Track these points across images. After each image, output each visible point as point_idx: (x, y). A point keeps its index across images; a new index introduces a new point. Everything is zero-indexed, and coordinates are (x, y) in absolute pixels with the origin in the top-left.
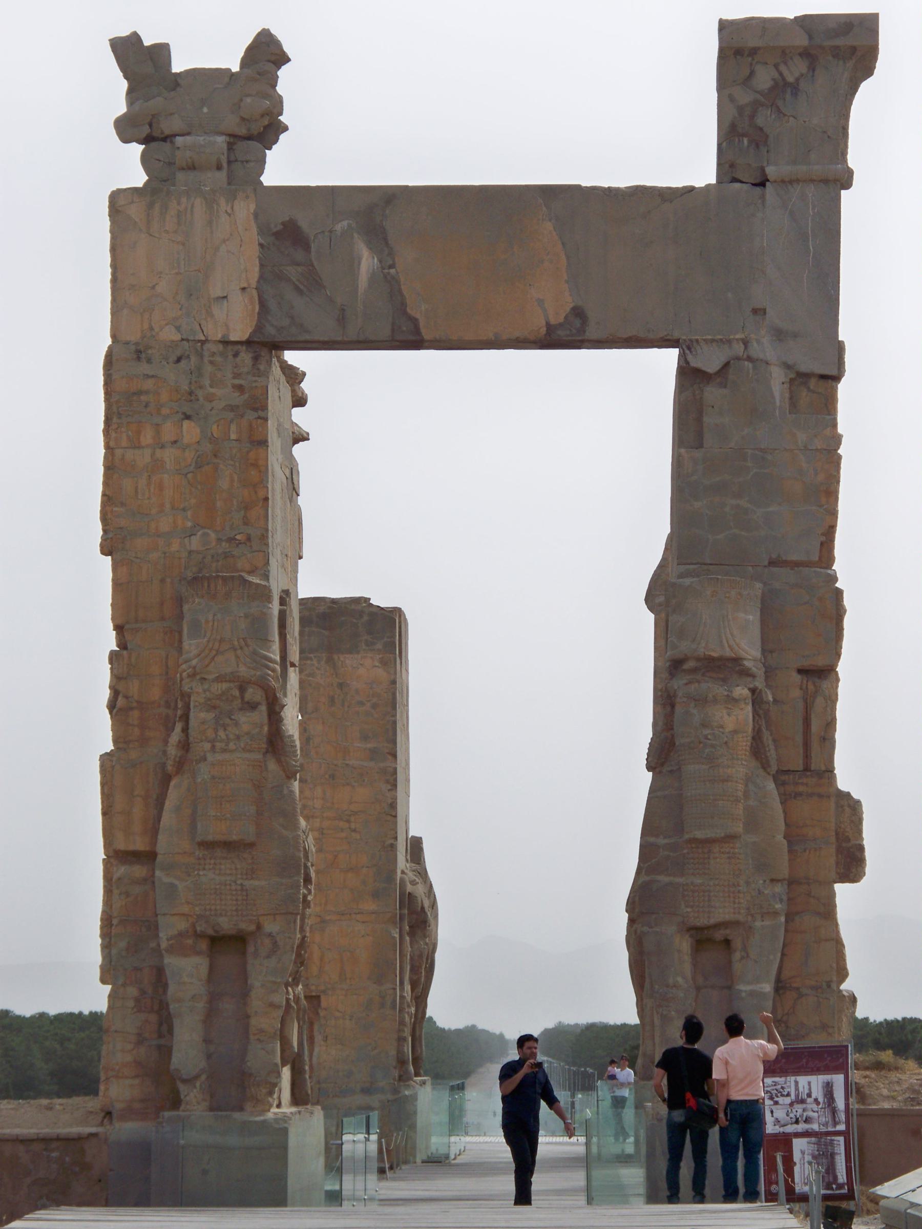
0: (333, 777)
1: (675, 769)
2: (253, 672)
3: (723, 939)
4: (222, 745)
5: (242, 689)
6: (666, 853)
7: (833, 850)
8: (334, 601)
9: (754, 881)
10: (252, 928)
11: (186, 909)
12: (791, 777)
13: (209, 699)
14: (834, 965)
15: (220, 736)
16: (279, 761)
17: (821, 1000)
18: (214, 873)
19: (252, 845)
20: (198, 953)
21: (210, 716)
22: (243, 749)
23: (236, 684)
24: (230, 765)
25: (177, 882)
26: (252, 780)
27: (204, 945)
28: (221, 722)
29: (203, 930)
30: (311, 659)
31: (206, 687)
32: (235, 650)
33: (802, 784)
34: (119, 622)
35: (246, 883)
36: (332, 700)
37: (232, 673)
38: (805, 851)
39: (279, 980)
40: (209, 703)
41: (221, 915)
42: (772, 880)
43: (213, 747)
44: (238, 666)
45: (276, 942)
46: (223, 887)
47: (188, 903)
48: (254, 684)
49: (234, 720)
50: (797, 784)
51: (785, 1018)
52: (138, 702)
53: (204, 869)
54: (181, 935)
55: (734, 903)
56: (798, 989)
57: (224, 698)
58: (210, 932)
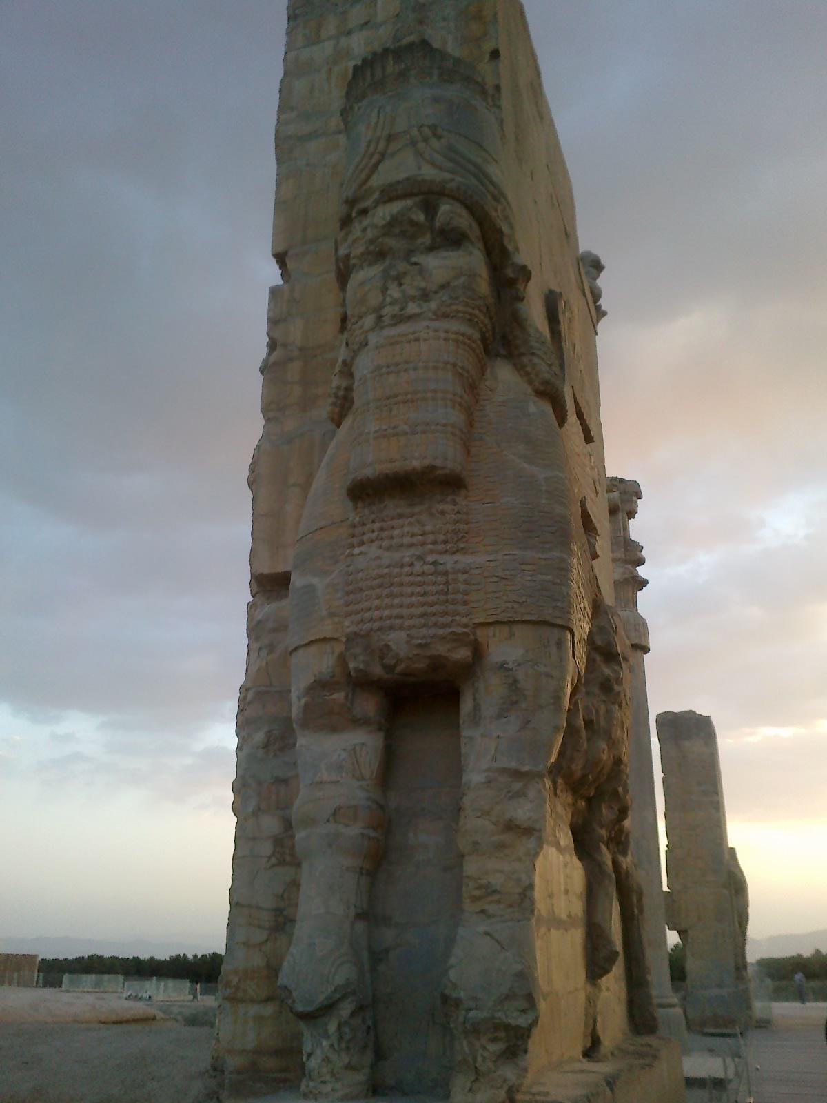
2: (447, 176)
4: (396, 309)
5: (430, 209)
8: (676, 713)
10: (463, 654)
11: (327, 630)
13: (372, 241)
15: (390, 296)
16: (520, 368)
18: (380, 547)
19: (452, 483)
20: (358, 722)
21: (375, 271)
22: (435, 313)
23: (417, 199)
24: (409, 342)
25: (315, 581)
26: (455, 365)
27: (369, 705)
28: (393, 273)
29: (361, 666)
31: (366, 222)
32: (413, 143)
34: (280, 249)
35: (449, 561)
37: (408, 179)
39: (526, 768)
40: (372, 248)
41: (391, 628)
43: (380, 318)
44: (420, 168)
45: (516, 681)
46: (396, 571)
47: (332, 615)
48: (449, 196)
49: (416, 264)
52: (301, 349)
53: (362, 543)
54: (321, 685)
57: (397, 230)
58: (377, 671)
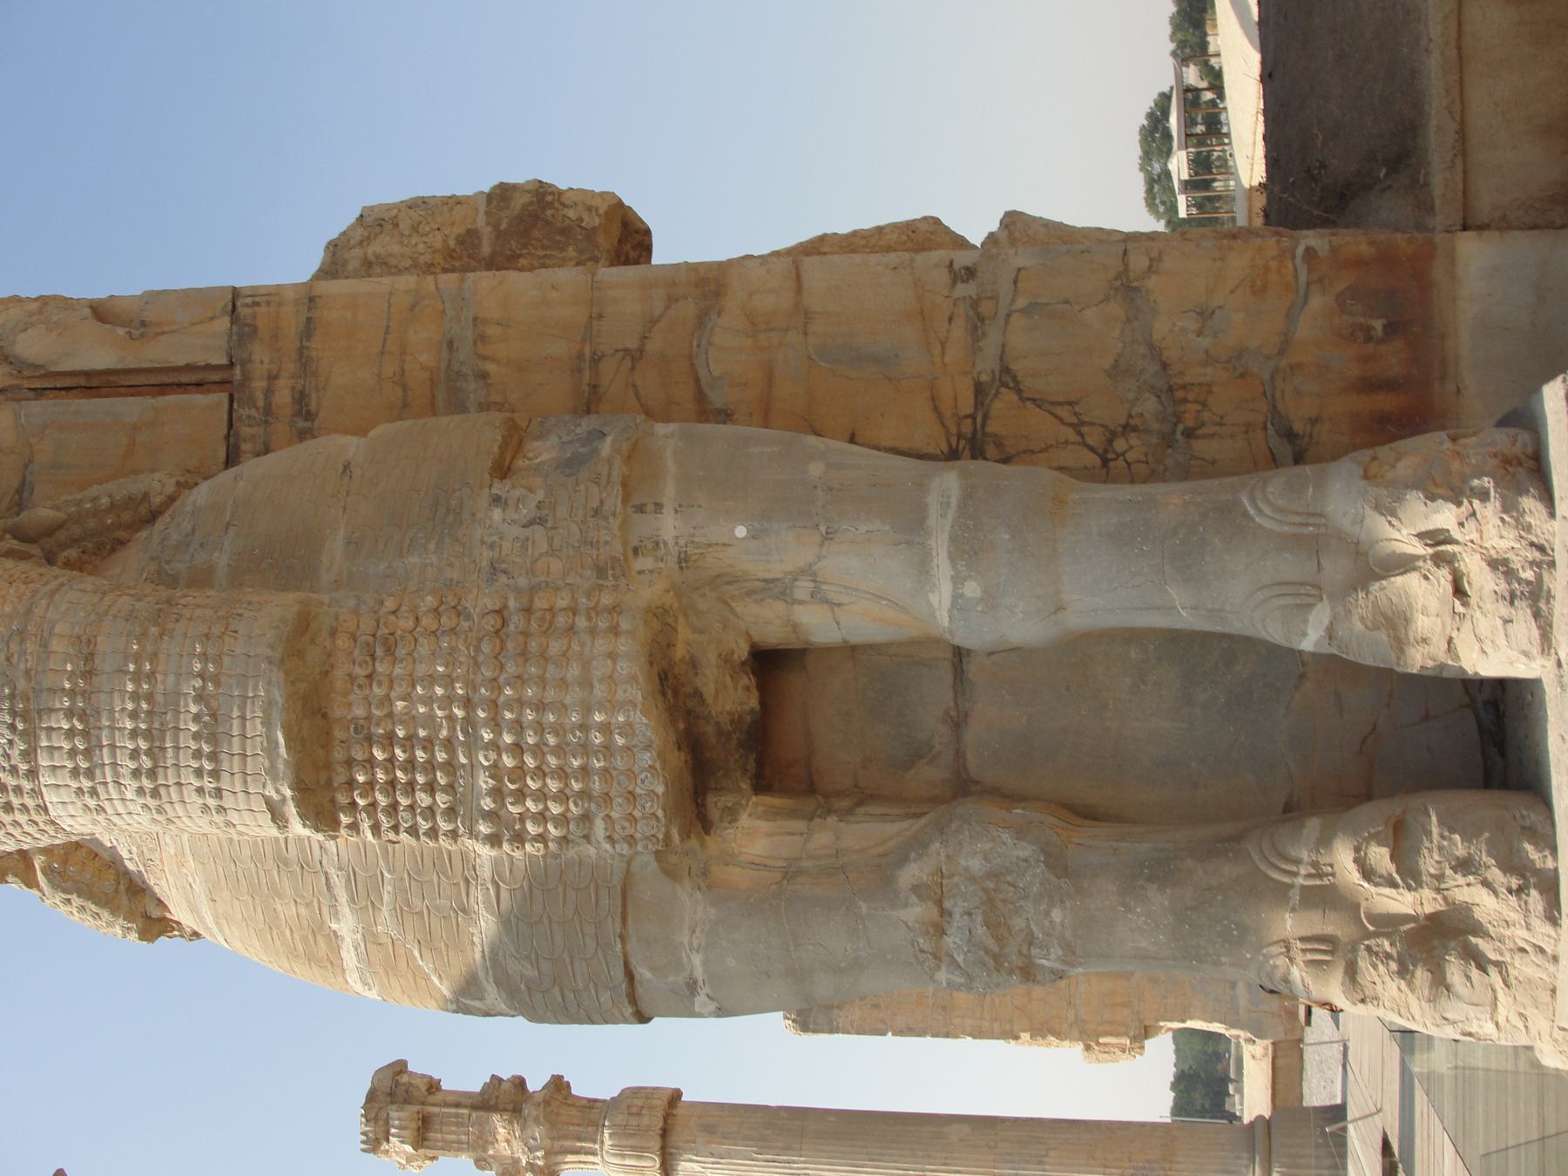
0: (944, 1008)
1: (134, 849)
3: (747, 680)
6: (385, 912)
7: (484, 280)
9: (492, 546)
12: (246, 431)
14: (892, 258)
17: (1021, 303)
30: (838, 1023)
33: (268, 393)
36: (876, 1006)
38: (484, 376)
42: (502, 470)
50: (268, 411)
51: (1095, 437)
55: (571, 629)
56: (979, 389)
